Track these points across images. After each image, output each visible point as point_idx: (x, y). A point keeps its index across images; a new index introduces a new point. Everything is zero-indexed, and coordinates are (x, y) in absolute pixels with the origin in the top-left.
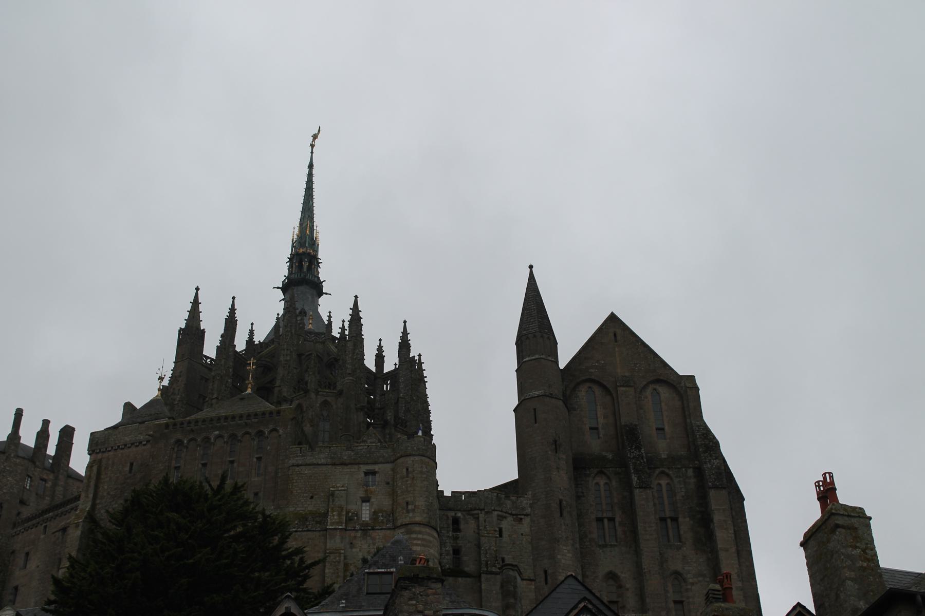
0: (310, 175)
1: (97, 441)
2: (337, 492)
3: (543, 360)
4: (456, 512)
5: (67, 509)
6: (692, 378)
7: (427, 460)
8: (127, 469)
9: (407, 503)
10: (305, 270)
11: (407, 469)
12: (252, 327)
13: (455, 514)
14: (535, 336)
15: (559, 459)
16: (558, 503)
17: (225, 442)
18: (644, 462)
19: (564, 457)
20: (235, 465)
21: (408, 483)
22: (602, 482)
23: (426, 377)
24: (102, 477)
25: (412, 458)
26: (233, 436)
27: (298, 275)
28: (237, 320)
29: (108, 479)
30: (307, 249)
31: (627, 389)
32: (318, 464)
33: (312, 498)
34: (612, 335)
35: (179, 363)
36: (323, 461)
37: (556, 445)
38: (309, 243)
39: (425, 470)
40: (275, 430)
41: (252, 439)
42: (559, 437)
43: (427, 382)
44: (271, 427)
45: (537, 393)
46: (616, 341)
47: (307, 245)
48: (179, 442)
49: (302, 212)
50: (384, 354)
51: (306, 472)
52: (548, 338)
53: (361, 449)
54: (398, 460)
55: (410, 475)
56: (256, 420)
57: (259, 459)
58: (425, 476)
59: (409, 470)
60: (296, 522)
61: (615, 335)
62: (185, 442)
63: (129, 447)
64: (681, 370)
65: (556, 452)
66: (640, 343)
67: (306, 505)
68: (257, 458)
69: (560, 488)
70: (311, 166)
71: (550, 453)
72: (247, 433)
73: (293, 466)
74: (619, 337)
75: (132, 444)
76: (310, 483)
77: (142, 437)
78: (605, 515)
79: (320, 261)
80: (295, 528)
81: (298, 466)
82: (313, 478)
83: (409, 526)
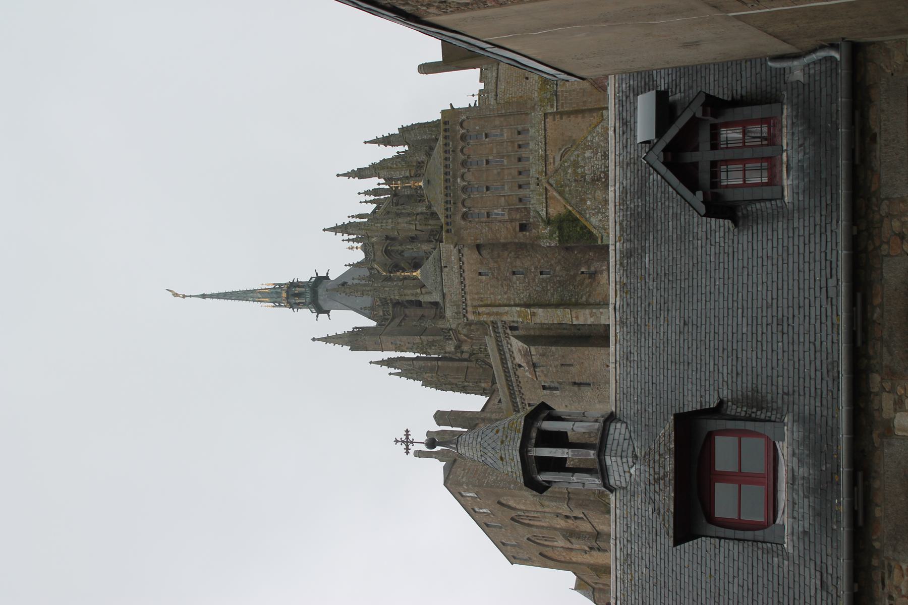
1: (456, 313)
5: (515, 381)
8: (484, 277)
17: (468, 171)
20: (490, 158)
24: (489, 302)
26: (464, 164)
29: (492, 296)
32: (497, 77)
33: (527, 78)
35: (383, 347)
36: (494, 74)
40: (461, 125)
41: (468, 145)
44: (458, 127)
48: (465, 216)
51: (503, 87)
56: (451, 143)
57: (487, 136)
60: (548, 87)
62: (464, 210)
63: (464, 279)
67: (534, 82)
68: (486, 138)
72: (462, 151)
73: (496, 99)
75: (461, 276)
77: (456, 267)
80: (553, 87)
81: (496, 95)
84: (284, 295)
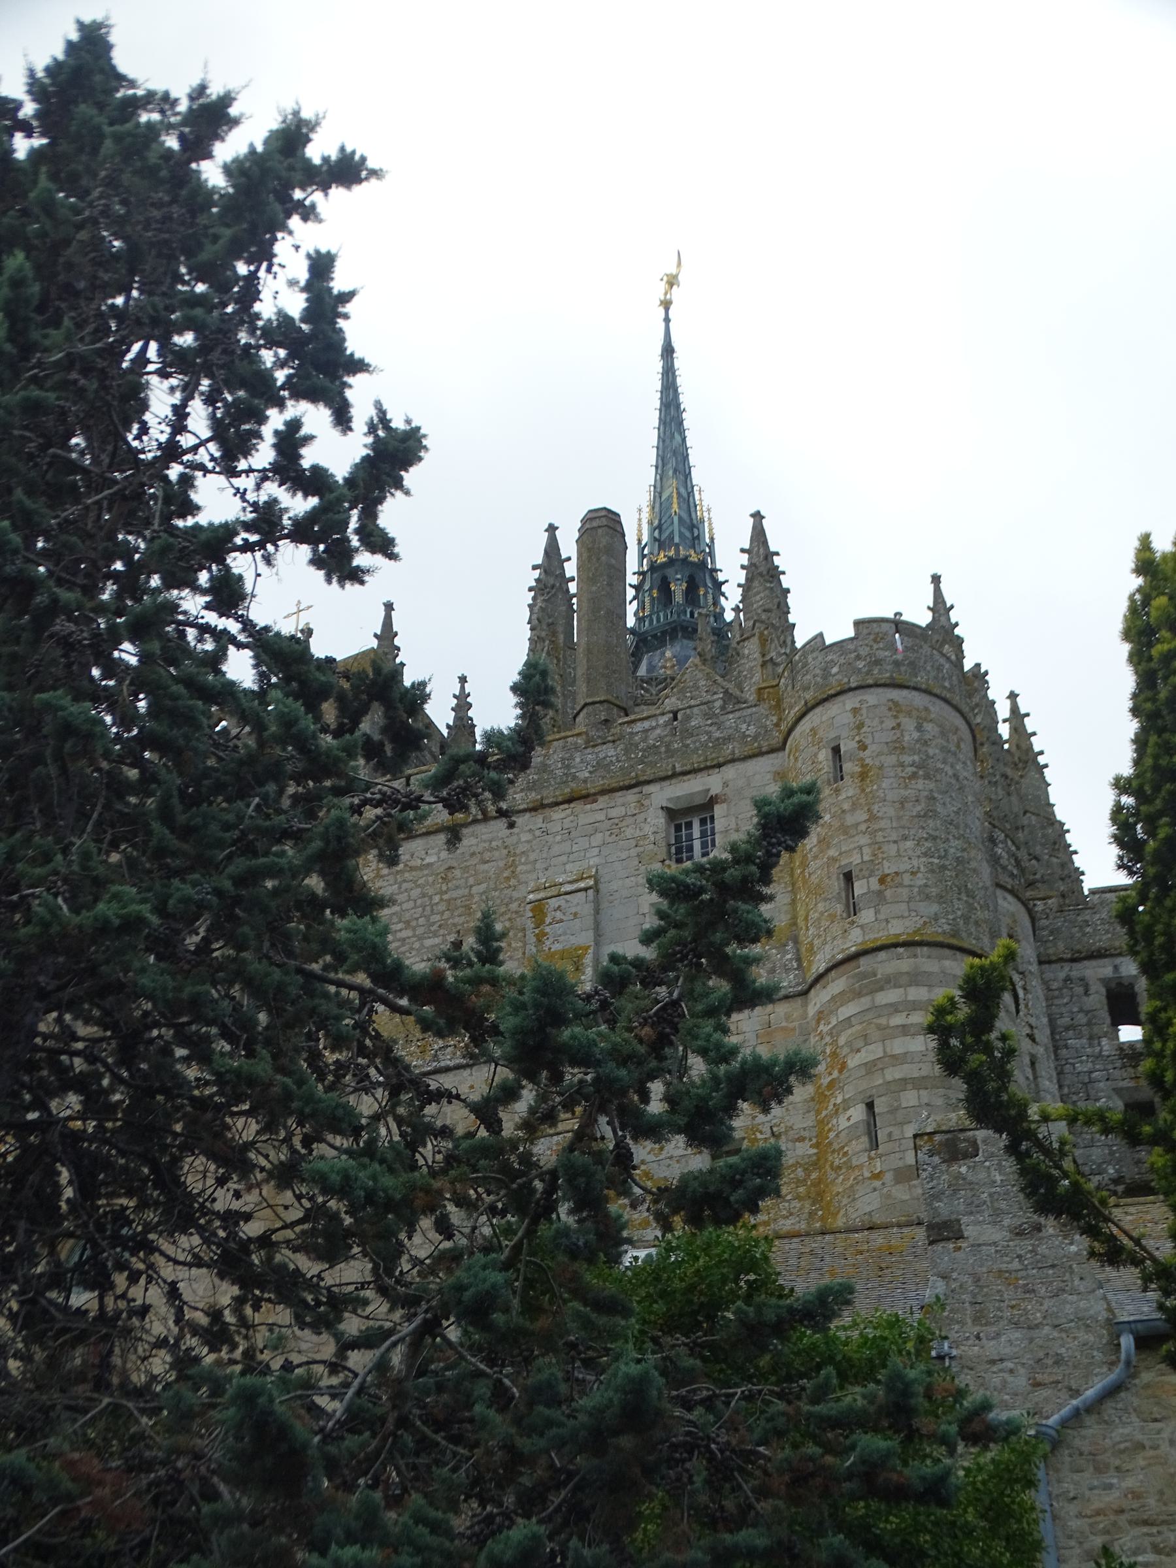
2: (554, 903)
4: (1118, 960)
7: (919, 699)
9: (848, 877)
10: (679, 598)
11: (836, 750)
12: (463, 688)
13: (1116, 968)
21: (843, 796)
23: (1041, 753)
28: (402, 665)
30: (677, 551)
38: (681, 535)
43: (1046, 766)
47: (677, 540)
51: (428, 860)
53: (646, 731)
54: (798, 730)
55: (848, 767)
70: (668, 351)
76: (445, 897)
79: (721, 577)
82: (457, 873)
83: (863, 961)
84: (662, 559)
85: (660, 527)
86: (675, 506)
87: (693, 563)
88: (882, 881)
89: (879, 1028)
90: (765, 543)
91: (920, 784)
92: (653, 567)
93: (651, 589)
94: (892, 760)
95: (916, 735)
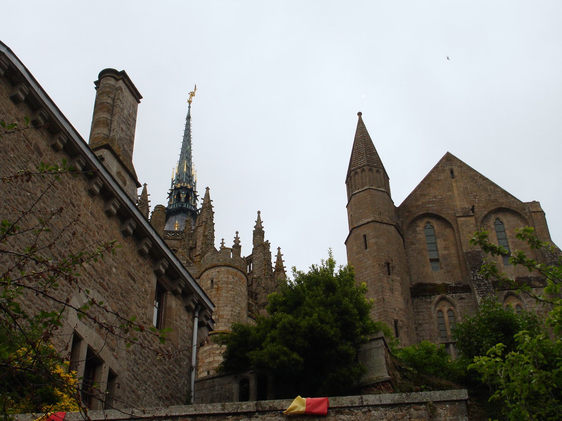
0: (188, 125)
3: (372, 190)
6: (536, 204)
10: (183, 200)
14: (363, 170)
15: (393, 281)
16: (393, 323)
18: (489, 283)
19: (399, 279)
22: (445, 309)
23: (285, 267)
25: (217, 269)
27: (175, 205)
30: (184, 184)
31: (468, 219)
34: (449, 172)
37: (388, 267)
38: (186, 179)
39: (231, 280)
42: (392, 260)
43: (286, 271)
45: (366, 221)
46: (453, 177)
47: (184, 181)
49: (181, 155)
50: (240, 244)
52: (378, 171)
54: (204, 274)
55: (215, 286)
58: (231, 286)
59: (214, 281)
61: (452, 172)
64: (524, 197)
65: (389, 274)
66: (478, 177)
69: (395, 308)
70: (189, 118)
71: (382, 275)
74: (456, 174)
78: (450, 341)
79: (197, 194)
84: (179, 186)
85: (179, 175)
86: (185, 169)
87: (188, 189)
88: (219, 316)
89: (213, 353)
90: (209, 197)
91: (231, 292)
92: (176, 189)
93: (174, 196)
94: (225, 285)
95: (232, 280)
